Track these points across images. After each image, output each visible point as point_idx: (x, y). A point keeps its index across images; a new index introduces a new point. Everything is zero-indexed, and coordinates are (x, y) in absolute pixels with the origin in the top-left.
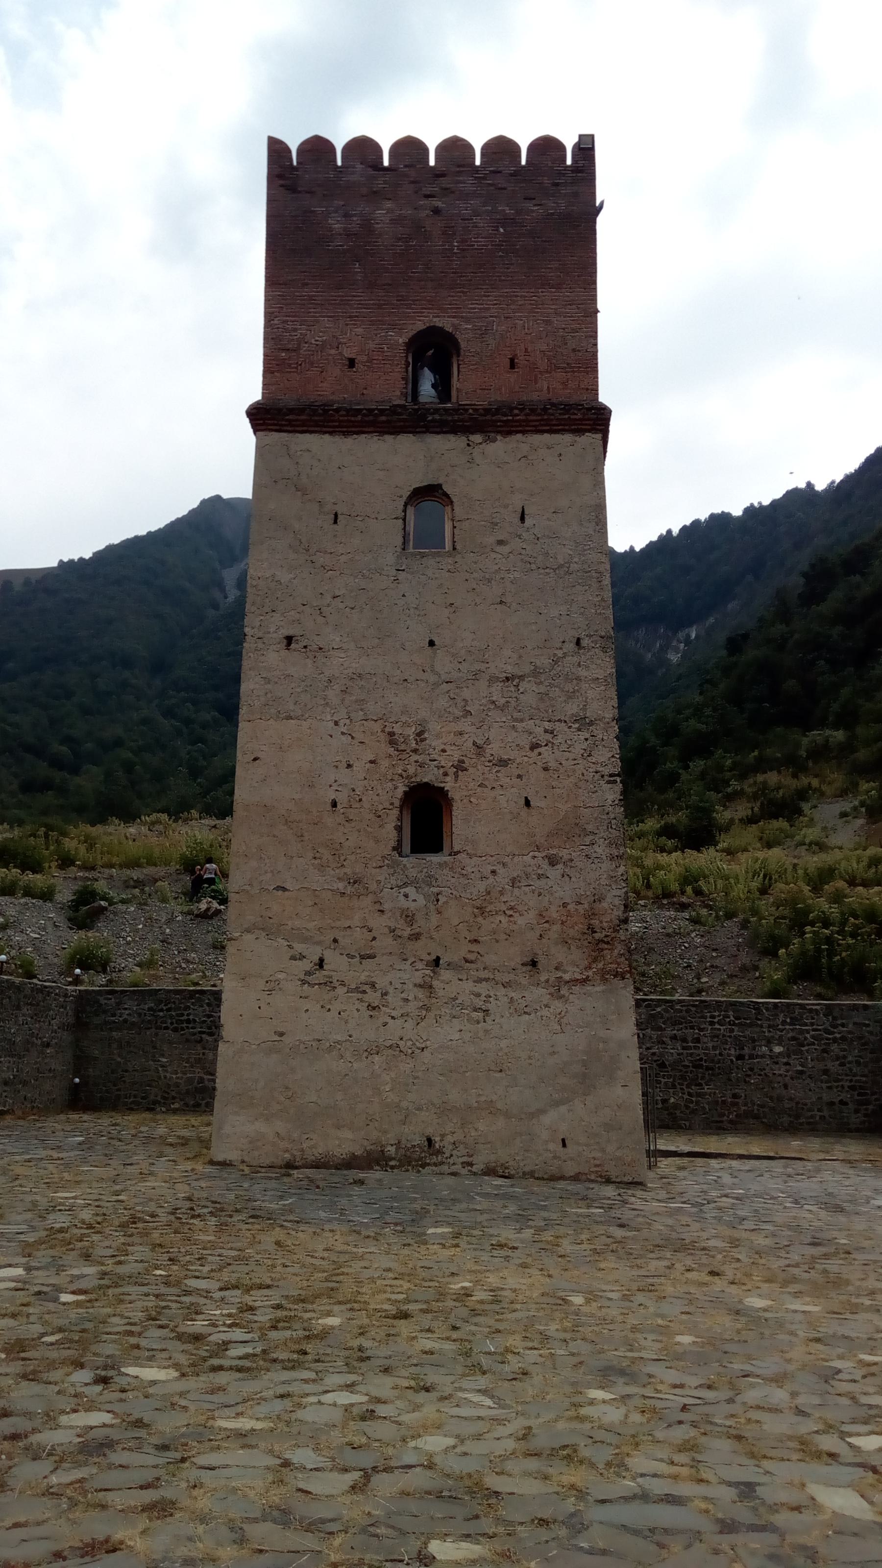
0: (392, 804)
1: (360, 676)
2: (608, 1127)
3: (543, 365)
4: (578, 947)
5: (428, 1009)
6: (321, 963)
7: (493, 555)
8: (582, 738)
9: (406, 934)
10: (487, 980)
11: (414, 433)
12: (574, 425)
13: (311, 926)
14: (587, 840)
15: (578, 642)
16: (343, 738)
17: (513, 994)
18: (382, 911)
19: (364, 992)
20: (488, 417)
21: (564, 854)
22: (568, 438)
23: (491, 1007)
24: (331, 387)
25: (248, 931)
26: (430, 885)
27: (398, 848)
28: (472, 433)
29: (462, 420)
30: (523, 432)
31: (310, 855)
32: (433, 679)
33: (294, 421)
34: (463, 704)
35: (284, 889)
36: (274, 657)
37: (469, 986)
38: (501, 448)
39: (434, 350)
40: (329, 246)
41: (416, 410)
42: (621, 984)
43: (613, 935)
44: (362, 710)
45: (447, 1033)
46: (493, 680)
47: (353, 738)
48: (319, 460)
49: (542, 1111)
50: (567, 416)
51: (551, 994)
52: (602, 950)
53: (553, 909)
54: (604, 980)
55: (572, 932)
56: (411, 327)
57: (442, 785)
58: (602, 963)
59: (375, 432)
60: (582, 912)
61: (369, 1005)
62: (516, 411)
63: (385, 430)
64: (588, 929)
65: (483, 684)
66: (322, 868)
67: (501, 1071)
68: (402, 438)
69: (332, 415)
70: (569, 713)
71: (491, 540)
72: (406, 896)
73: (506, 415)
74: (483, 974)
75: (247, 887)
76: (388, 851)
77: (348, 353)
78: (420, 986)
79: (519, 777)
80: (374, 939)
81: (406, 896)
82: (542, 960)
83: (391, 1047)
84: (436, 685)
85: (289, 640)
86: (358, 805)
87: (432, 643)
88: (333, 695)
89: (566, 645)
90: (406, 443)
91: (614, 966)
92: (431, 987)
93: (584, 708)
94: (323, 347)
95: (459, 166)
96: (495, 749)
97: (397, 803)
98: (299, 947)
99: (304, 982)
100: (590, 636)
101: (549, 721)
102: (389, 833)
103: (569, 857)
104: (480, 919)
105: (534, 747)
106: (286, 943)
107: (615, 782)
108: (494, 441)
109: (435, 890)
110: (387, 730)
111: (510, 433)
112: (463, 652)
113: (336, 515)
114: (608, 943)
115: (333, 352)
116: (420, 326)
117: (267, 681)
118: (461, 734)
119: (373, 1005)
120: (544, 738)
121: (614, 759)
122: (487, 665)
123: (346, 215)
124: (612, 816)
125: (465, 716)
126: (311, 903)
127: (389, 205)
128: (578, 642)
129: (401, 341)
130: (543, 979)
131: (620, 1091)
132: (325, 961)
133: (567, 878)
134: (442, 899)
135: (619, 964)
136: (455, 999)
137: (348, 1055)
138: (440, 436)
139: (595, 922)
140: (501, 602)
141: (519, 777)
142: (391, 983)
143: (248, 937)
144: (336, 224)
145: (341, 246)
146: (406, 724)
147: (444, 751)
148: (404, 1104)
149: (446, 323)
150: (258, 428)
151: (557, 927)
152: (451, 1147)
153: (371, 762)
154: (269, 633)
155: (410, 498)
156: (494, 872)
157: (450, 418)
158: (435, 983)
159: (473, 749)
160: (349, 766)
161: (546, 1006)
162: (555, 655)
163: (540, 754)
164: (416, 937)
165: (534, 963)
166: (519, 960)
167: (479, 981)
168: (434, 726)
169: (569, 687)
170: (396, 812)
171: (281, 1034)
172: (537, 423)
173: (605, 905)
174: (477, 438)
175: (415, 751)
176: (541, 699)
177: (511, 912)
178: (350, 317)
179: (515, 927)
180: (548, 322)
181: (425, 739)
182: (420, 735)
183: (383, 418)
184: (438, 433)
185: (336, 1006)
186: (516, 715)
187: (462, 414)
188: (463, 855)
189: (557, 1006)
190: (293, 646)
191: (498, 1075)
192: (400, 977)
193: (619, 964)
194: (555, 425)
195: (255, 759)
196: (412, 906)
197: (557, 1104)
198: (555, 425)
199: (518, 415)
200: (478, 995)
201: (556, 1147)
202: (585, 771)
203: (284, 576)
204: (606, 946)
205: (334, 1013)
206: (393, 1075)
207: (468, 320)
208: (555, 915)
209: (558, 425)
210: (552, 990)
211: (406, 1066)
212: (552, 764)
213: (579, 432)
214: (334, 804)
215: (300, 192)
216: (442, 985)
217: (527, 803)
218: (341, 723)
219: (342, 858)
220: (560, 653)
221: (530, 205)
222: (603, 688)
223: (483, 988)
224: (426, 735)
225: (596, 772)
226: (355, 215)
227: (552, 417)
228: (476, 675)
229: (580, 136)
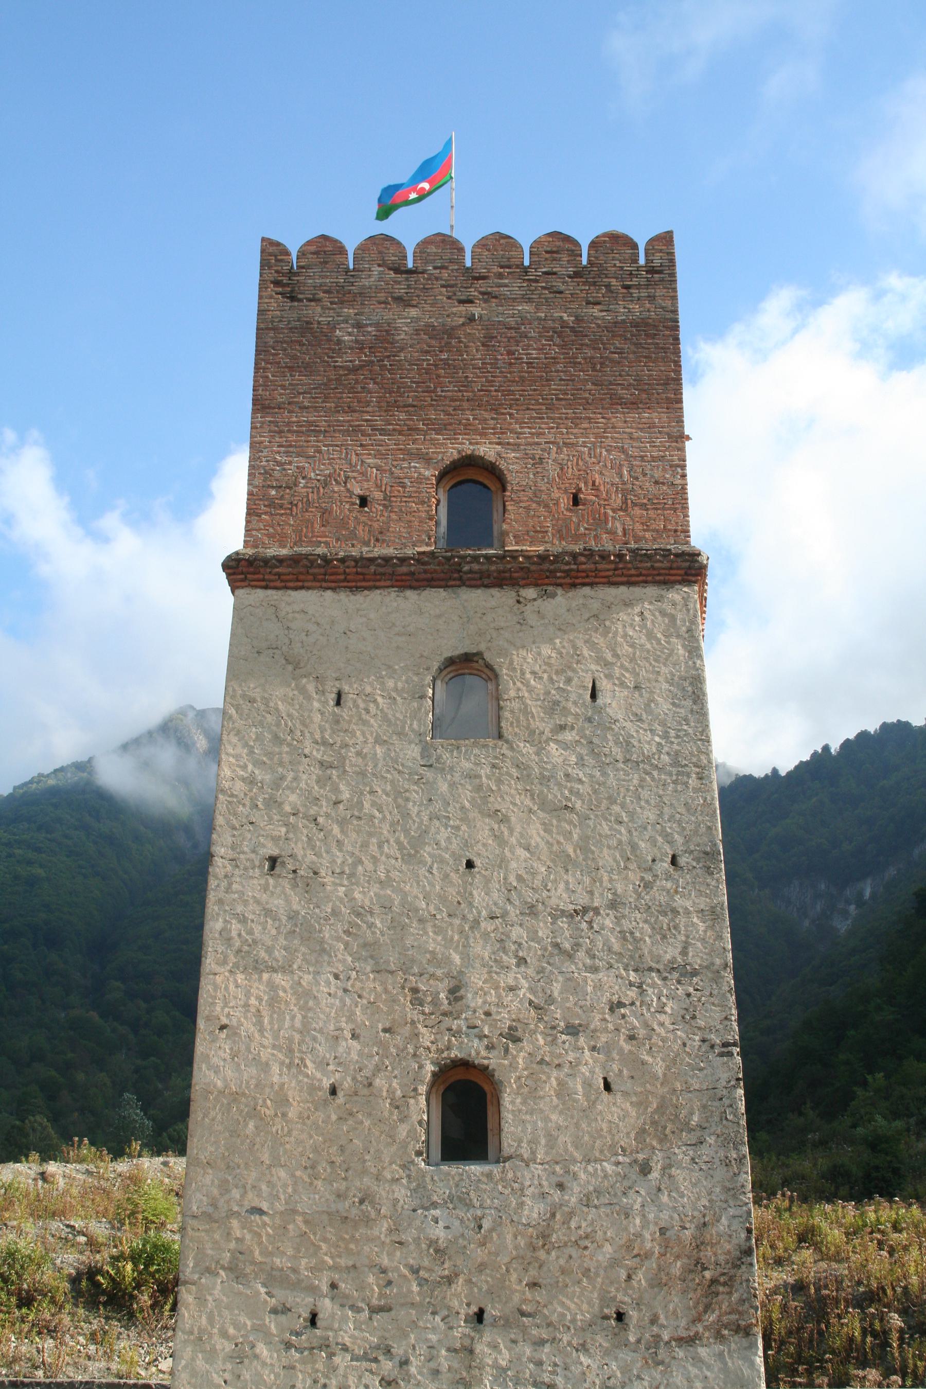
6: (313, 1320)
11: (446, 587)
12: (659, 575)
15: (674, 861)
19: (376, 1360)
20: (546, 566)
28: (523, 586)
30: (591, 585)
33: (284, 574)
39: (474, 482)
40: (337, 362)
41: (448, 559)
43: (732, 1272)
44: (372, 957)
48: (318, 624)
50: (649, 565)
52: (717, 1294)
54: (719, 1337)
57: (486, 1062)
58: (717, 1312)
59: (393, 587)
61: (382, 1379)
63: (408, 583)
64: (696, 1266)
68: (429, 593)
69: (335, 567)
73: (568, 563)
80: (389, 1283)
85: (273, 861)
86: (365, 1091)
87: (470, 865)
90: (435, 601)
91: (734, 1317)
92: (471, 1352)
93: (684, 952)
95: (502, 267)
104: (542, 1254)
108: (553, 596)
111: (574, 586)
114: (725, 1284)
119: (387, 1378)
123: (359, 326)
124: (727, 1102)
127: (413, 312)
132: (320, 1316)
135: (740, 1313)
138: (479, 591)
139: (708, 1254)
144: (344, 335)
145: (351, 361)
149: (487, 450)
150: (238, 584)
155: (440, 670)
157: (493, 568)
168: (476, 979)
172: (610, 573)
174: (530, 593)
178: (361, 445)
181: (461, 998)
182: (455, 993)
183: (404, 569)
184: (477, 587)
187: (509, 562)
190: (278, 870)
193: (740, 1313)
198: (632, 576)
199: (585, 564)
204: (721, 1289)
207: (516, 447)
209: (638, 576)
212: (642, 1033)
214: (333, 1091)
215: (300, 300)
221: (595, 311)
224: (462, 992)
226: (367, 325)
227: (630, 566)
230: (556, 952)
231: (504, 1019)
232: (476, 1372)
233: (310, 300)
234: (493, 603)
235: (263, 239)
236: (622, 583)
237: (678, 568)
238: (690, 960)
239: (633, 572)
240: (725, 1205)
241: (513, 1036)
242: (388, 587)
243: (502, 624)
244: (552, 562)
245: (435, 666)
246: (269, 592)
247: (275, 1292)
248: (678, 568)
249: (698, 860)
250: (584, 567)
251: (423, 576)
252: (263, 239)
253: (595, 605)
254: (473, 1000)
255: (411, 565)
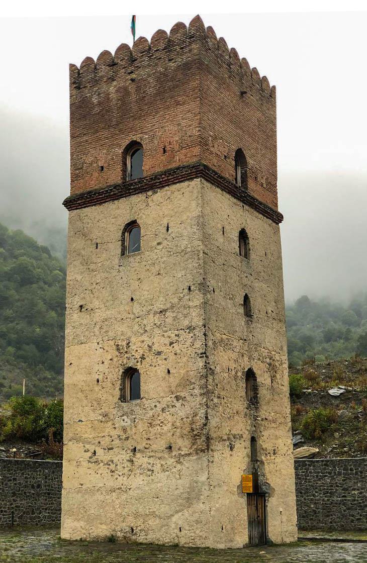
0: (118, 378)
1: (106, 320)
2: (197, 522)
3: (177, 148)
4: (187, 439)
5: (132, 472)
6: (95, 453)
7: (156, 251)
8: (190, 336)
9: (124, 437)
10: (152, 457)
12: (189, 176)
13: (91, 436)
14: (191, 387)
15: (189, 289)
16: (101, 350)
17: (162, 462)
18: (115, 428)
19: (110, 465)
21: (182, 394)
22: (186, 183)
23: (154, 468)
24: (94, 183)
25: (70, 440)
26: (132, 415)
27: (123, 398)
28: (148, 191)
29: (143, 186)
31: (90, 405)
32: (132, 316)
34: (144, 327)
35: (82, 421)
36: (75, 316)
37: (146, 460)
38: (159, 196)
42: (204, 455)
44: (107, 336)
45: (138, 481)
46: (155, 313)
47: (104, 349)
49: (172, 515)
51: (177, 462)
53: (178, 421)
54: (197, 454)
55: (185, 432)
56: (124, 144)
57: (136, 367)
60: (189, 422)
62: (163, 176)
65: (151, 315)
66: (94, 410)
67: (157, 498)
70: (185, 325)
71: (155, 243)
72: (124, 420)
74: (151, 454)
75: (69, 422)
76: (116, 399)
77: (100, 164)
78: (129, 461)
79: (165, 359)
80: (113, 441)
81: (124, 420)
82: (173, 445)
83: (118, 489)
84: (134, 319)
85: (81, 306)
87: (132, 299)
88: (96, 330)
89: (184, 291)
92: (132, 461)
93: (191, 322)
94: (91, 164)
96: (156, 348)
97: (120, 377)
98: (87, 446)
99: (89, 462)
100: (194, 284)
101: (177, 330)
102: (117, 393)
103: (184, 396)
104: (150, 429)
105: (171, 343)
106: (83, 445)
107: (203, 357)
108: (157, 192)
109: (134, 416)
110: (116, 344)
111: (163, 187)
112: (144, 301)
113: (97, 244)
114: (198, 436)
115: (95, 165)
116: (128, 142)
117: (74, 327)
118: (143, 342)
120: (175, 338)
121: (202, 346)
122: (153, 306)
125: (144, 333)
126: (90, 426)
127: (115, 83)
128: (189, 289)
129: (120, 152)
130: (173, 454)
131: (201, 505)
133: (183, 406)
134: (137, 421)
135: (203, 445)
136: (141, 466)
137: (104, 492)
139: (194, 426)
140: (159, 274)
141: (165, 359)
142: (119, 460)
143: (70, 443)
144: (95, 100)
146: (123, 340)
147: (137, 351)
148: (123, 513)
151: (179, 430)
152: (139, 532)
153: (110, 360)
154: (74, 305)
156: (155, 406)
158: (134, 459)
159: (148, 348)
160: (103, 363)
161: (175, 467)
162: (180, 297)
163: (173, 347)
164: (127, 438)
165: (170, 448)
166: (164, 446)
167: (150, 457)
168: (133, 340)
169: (185, 312)
170: (119, 382)
171: (82, 485)
172: (173, 180)
173: (198, 418)
174: (150, 193)
175: (126, 352)
176: (174, 320)
177: (161, 425)
179: (163, 431)
180: (179, 125)
181: (130, 346)
183: (112, 193)
185: (100, 472)
186: (164, 329)
187: (142, 183)
188: (144, 399)
189: (179, 466)
191: (157, 500)
192: (121, 457)
193: (203, 445)
194: (180, 179)
195: (71, 364)
196: (126, 424)
197: (177, 512)
198: (180, 179)
199: (164, 178)
200: (150, 464)
201: (177, 531)
202: (191, 353)
203: (79, 277)
205: (99, 474)
206: (119, 501)
208: (178, 424)
210: (177, 459)
211: (124, 497)
212: (178, 352)
213: (192, 179)
214: (98, 381)
216: (137, 460)
217: (169, 372)
218: (100, 343)
219: (101, 405)
220: (182, 295)
222: (199, 310)
223: (151, 461)
224: (130, 344)
225: (196, 353)
228: (149, 312)
229: (197, 20)
230: (155, 327)
231: (141, 352)
232: (134, 467)
233: (84, 87)
234: (139, 199)
235: (70, 64)
236: (177, 183)
237: (193, 172)
238: (193, 324)
239: (180, 177)
240: (199, 409)
241: (143, 358)
242: (109, 201)
243: (142, 208)
244: (155, 180)
245: (122, 228)
246: (78, 210)
247: (86, 445)
248: (193, 172)
249: (196, 287)
250: (164, 179)
251: (119, 194)
252: (70, 64)
253: (169, 193)
254: (133, 347)
255: (114, 191)
